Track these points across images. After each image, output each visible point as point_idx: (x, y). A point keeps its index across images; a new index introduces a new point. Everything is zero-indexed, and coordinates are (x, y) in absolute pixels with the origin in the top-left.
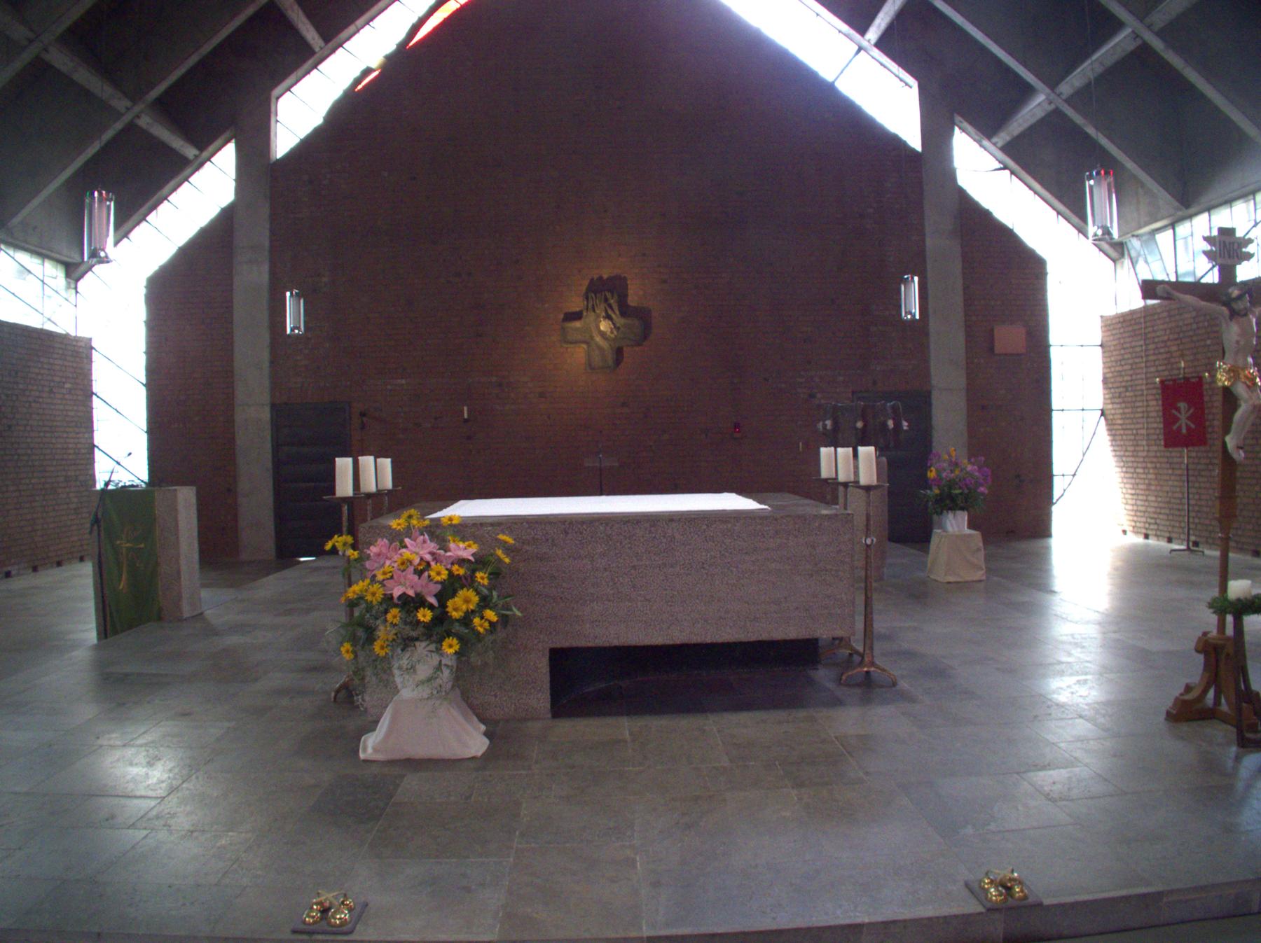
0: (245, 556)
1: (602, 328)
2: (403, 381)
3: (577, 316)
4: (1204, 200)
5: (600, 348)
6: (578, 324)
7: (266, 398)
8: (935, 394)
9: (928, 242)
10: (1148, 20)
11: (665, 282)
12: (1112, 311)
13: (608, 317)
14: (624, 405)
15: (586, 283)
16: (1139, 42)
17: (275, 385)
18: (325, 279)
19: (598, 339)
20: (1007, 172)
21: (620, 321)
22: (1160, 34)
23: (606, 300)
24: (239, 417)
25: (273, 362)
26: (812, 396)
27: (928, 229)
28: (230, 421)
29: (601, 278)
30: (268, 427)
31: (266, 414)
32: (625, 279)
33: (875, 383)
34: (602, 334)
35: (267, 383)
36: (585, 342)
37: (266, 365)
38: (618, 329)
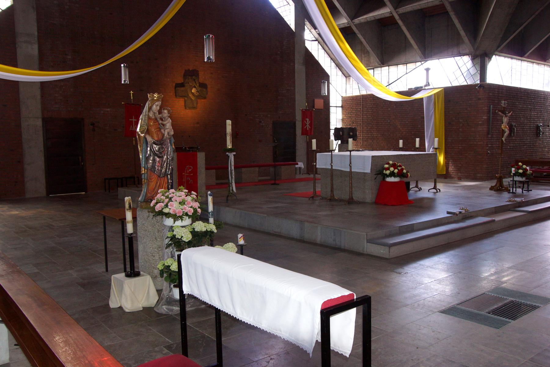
0: (28, 196)
1: (193, 91)
2: (109, 110)
3: (182, 85)
4: (390, 63)
5: (191, 99)
6: (182, 89)
7: (39, 114)
8: (297, 122)
9: (296, 66)
10: (397, 10)
11: (212, 74)
12: (344, 95)
13: (195, 87)
14: (198, 123)
15: (184, 71)
16: (391, 15)
17: (44, 108)
18: (70, 57)
19: (190, 95)
20: (317, 42)
21: (199, 89)
22: (399, 15)
23: (194, 80)
24: (24, 125)
25: (42, 96)
26: (260, 122)
27: (296, 61)
28: (19, 126)
29: (189, 70)
30: (41, 129)
31: (39, 123)
32: (198, 71)
33: (279, 117)
34: (193, 94)
35: (39, 106)
36: (185, 97)
37: (39, 97)
38: (198, 92)
